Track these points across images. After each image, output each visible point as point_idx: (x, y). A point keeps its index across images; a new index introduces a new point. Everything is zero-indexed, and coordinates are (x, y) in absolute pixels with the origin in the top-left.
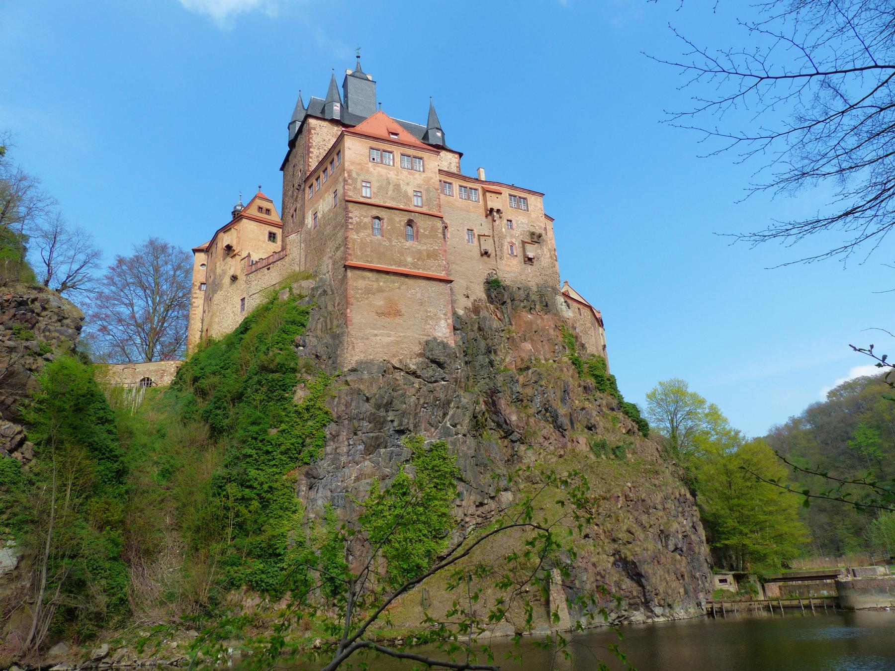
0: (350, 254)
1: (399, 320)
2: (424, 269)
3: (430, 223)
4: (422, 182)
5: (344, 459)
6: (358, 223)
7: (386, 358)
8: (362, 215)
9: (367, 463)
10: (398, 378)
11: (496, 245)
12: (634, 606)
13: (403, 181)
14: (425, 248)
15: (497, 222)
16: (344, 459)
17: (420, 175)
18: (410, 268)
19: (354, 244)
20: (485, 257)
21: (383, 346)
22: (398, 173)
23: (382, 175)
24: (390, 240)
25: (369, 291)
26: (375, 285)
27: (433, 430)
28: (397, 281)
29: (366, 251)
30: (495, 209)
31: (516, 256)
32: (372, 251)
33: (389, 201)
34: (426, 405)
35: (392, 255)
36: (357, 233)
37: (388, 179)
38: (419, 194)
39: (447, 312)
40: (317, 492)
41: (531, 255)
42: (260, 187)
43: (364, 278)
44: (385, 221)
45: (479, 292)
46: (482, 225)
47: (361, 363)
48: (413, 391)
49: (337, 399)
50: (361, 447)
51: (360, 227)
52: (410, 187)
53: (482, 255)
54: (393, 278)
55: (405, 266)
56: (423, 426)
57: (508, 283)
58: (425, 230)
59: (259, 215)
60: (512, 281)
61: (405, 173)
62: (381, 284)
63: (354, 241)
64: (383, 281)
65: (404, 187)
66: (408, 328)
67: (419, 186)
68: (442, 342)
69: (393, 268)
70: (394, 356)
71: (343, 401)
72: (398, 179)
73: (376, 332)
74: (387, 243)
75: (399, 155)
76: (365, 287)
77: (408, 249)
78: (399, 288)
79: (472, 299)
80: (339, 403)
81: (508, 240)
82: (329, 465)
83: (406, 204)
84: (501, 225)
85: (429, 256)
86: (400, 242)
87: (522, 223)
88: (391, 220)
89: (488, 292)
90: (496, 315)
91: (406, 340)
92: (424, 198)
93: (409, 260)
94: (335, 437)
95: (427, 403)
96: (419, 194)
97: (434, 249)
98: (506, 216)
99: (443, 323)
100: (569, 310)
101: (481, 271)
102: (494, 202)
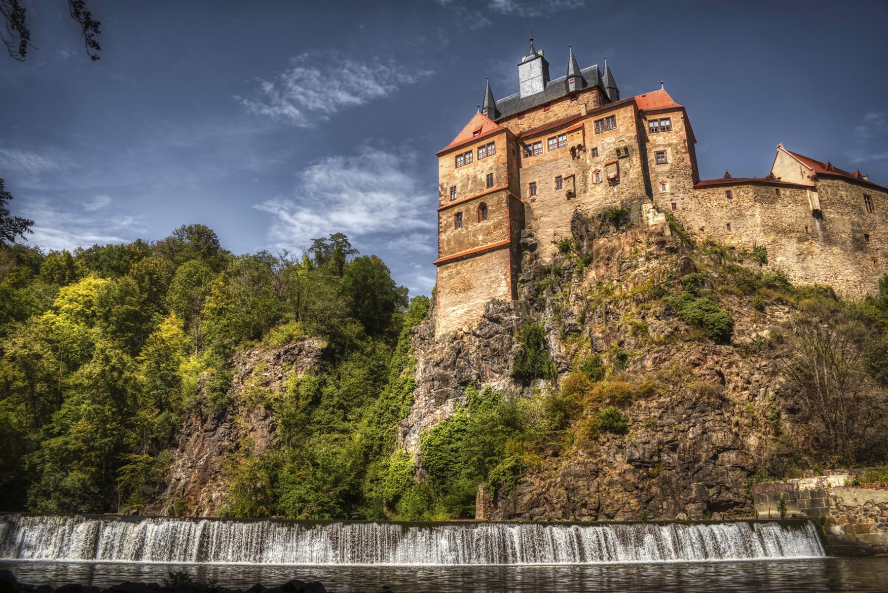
1: (470, 293)
6: (445, 225)
7: (460, 327)
9: (438, 412)
14: (492, 222)
15: (581, 157)
16: (423, 411)
25: (451, 277)
26: (454, 271)
27: (498, 375)
31: (601, 182)
37: (468, 175)
44: (463, 214)
45: (566, 233)
46: (567, 167)
48: (474, 348)
50: (433, 401)
51: (448, 226)
55: (478, 245)
58: (492, 206)
61: (480, 163)
62: (459, 268)
63: (443, 240)
65: (479, 177)
67: (491, 168)
69: (470, 250)
74: (464, 232)
81: (593, 169)
87: (609, 144)
88: (467, 210)
91: (475, 308)
93: (481, 238)
99: (504, 283)
100: (660, 214)
101: (568, 210)
102: (576, 140)
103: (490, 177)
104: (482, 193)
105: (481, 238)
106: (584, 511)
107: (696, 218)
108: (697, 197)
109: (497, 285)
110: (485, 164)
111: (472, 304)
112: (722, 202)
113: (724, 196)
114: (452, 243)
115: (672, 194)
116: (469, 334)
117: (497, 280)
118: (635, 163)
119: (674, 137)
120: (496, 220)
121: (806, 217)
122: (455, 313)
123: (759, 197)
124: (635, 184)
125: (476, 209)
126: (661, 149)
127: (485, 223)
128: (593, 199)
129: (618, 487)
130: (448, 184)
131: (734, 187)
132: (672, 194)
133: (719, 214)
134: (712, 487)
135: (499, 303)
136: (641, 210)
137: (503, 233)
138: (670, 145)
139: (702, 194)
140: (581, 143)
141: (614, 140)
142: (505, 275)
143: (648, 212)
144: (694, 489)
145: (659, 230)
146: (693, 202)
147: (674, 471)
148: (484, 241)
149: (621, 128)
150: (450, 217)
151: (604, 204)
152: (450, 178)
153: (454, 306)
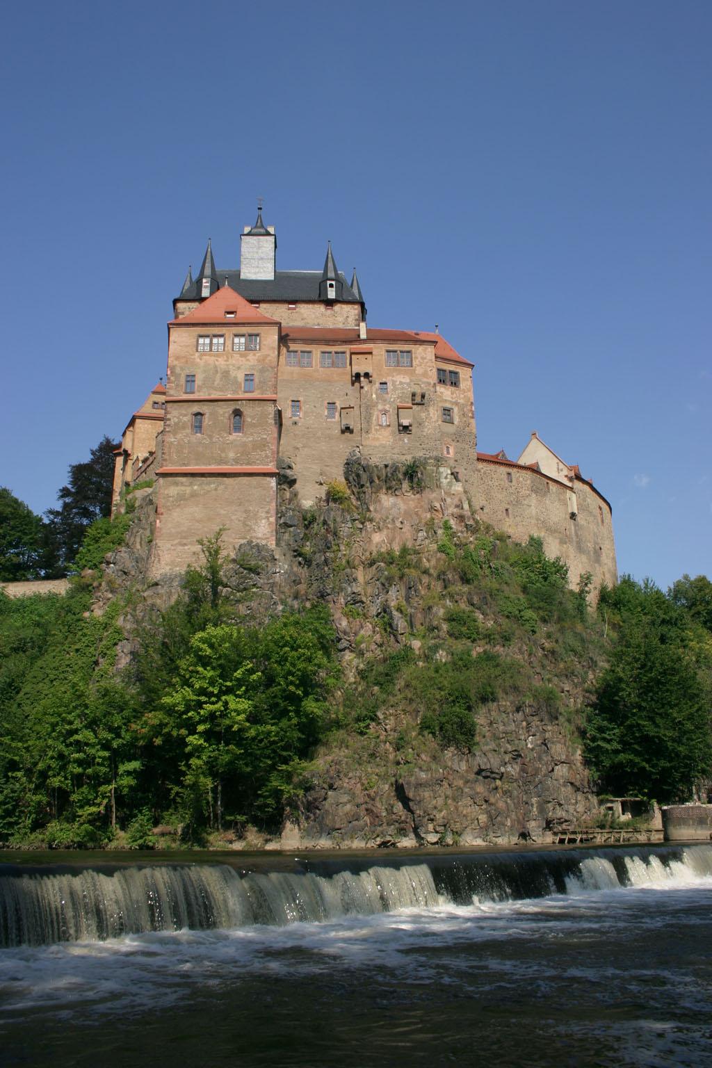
0: (165, 460)
2: (248, 464)
3: (259, 409)
4: (256, 363)
6: (176, 424)
12: (402, 832)
13: (234, 365)
15: (366, 389)
17: (254, 355)
18: (232, 465)
19: (170, 448)
20: (347, 434)
22: (228, 357)
23: (209, 364)
24: (211, 437)
26: (188, 490)
28: (213, 483)
30: (362, 374)
32: (189, 453)
33: (215, 392)
35: (212, 453)
39: (269, 509)
41: (405, 422)
42: (161, 379)
43: (176, 484)
44: (206, 416)
51: (178, 427)
53: (343, 432)
55: (226, 463)
59: (155, 411)
62: (195, 487)
64: (197, 485)
65: (233, 374)
67: (253, 367)
68: (257, 545)
72: (227, 365)
75: (232, 336)
76: (178, 494)
77: (232, 443)
81: (380, 407)
87: (401, 383)
97: (262, 439)
98: (375, 377)
101: (343, 449)
102: (361, 365)
103: (249, 378)
105: (231, 455)
106: (431, 827)
108: (479, 471)
112: (502, 483)
113: (505, 477)
114: (186, 451)
115: (456, 461)
119: (462, 396)
121: (566, 519)
123: (534, 487)
125: (227, 415)
126: (448, 405)
127: (235, 436)
131: (515, 470)
132: (456, 461)
133: (500, 496)
134: (549, 802)
137: (267, 457)
138: (457, 404)
140: (370, 370)
142: (267, 512)
144: (535, 806)
146: (476, 475)
147: (515, 784)
148: (236, 461)
149: (418, 368)
150: (185, 415)
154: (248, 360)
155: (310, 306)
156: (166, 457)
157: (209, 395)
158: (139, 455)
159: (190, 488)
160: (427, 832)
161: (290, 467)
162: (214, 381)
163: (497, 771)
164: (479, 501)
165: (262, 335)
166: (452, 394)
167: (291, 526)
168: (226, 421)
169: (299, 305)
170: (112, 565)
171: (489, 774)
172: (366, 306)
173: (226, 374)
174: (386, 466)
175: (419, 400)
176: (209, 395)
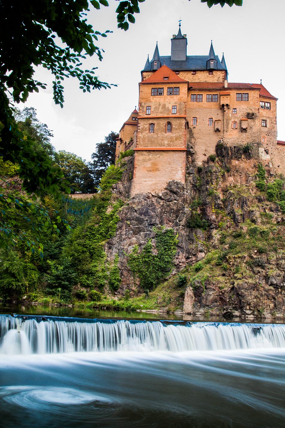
0: (137, 144)
4: (177, 100)
5: (124, 237)
6: (142, 129)
7: (149, 192)
8: (145, 124)
9: (134, 238)
10: (153, 200)
11: (225, 124)
12: (236, 309)
15: (227, 112)
17: (177, 97)
18: (166, 146)
19: (140, 139)
21: (149, 186)
23: (157, 102)
24: (157, 134)
25: (144, 161)
26: (147, 158)
27: (171, 223)
29: (145, 141)
30: (225, 104)
31: (237, 129)
32: (148, 141)
33: (159, 114)
34: (166, 212)
35: (158, 141)
36: (142, 133)
37: (159, 103)
38: (175, 107)
40: (113, 250)
41: (244, 127)
43: (142, 155)
44: (155, 125)
45: (212, 152)
46: (216, 115)
47: (138, 194)
49: (122, 212)
51: (144, 130)
52: (170, 104)
54: (156, 153)
55: (164, 146)
56: (165, 222)
57: (228, 146)
60: (232, 143)
62: (150, 156)
65: (167, 106)
66: (162, 177)
68: (177, 182)
69: (158, 148)
70: (153, 190)
71: (124, 212)
72: (165, 102)
73: (146, 180)
74: (156, 136)
77: (166, 137)
78: (159, 157)
79: (208, 156)
80: (123, 213)
81: (233, 120)
82: (117, 239)
83: (168, 114)
84: (229, 113)
85: (176, 139)
86: (162, 134)
89: (217, 151)
90: (219, 164)
92: (178, 109)
94: (120, 228)
95: (166, 211)
96: (175, 107)
98: (231, 107)
101: (214, 140)
102: (224, 101)
104: (168, 116)
105: (166, 142)
107: (277, 160)
108: (278, 149)
109: (175, 172)
110: (172, 99)
111: (158, 180)
114: (146, 140)
115: (267, 144)
116: (156, 197)
117: (177, 170)
118: (256, 123)
119: (271, 114)
120: (177, 134)
122: (146, 182)
124: (256, 135)
125: (164, 124)
126: (264, 118)
127: (168, 134)
128: (230, 137)
129: (266, 297)
130: (145, 104)
132: (267, 144)
135: (177, 183)
136: (258, 150)
137: (182, 143)
139: (281, 148)
141: (246, 107)
143: (262, 153)
145: (267, 164)
146: (276, 151)
148: (169, 145)
149: (251, 102)
150: (146, 125)
151: (237, 142)
152: (147, 101)
153: (146, 178)
154: (173, 99)
155: (202, 72)
156: (138, 143)
157: (157, 115)
158: (127, 141)
159: (148, 157)
160: (246, 309)
161: (192, 148)
162: (159, 109)
163: (279, 285)
164: (277, 162)
165: (180, 87)
166: (267, 113)
167: (191, 174)
168: (164, 127)
169: (197, 72)
170: (115, 189)
171: (275, 286)
172: (228, 72)
173: (164, 106)
174: (235, 147)
175: (250, 116)
176: (157, 115)
